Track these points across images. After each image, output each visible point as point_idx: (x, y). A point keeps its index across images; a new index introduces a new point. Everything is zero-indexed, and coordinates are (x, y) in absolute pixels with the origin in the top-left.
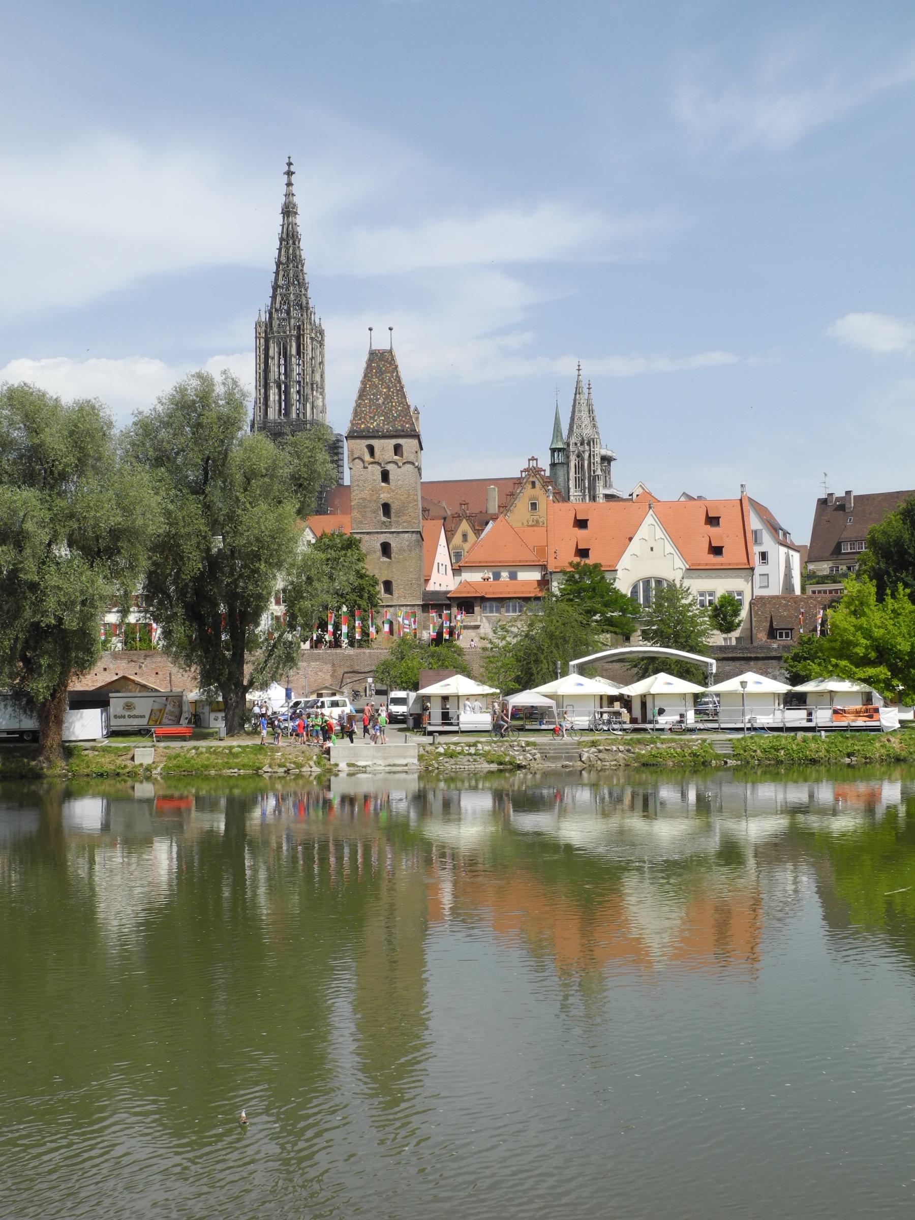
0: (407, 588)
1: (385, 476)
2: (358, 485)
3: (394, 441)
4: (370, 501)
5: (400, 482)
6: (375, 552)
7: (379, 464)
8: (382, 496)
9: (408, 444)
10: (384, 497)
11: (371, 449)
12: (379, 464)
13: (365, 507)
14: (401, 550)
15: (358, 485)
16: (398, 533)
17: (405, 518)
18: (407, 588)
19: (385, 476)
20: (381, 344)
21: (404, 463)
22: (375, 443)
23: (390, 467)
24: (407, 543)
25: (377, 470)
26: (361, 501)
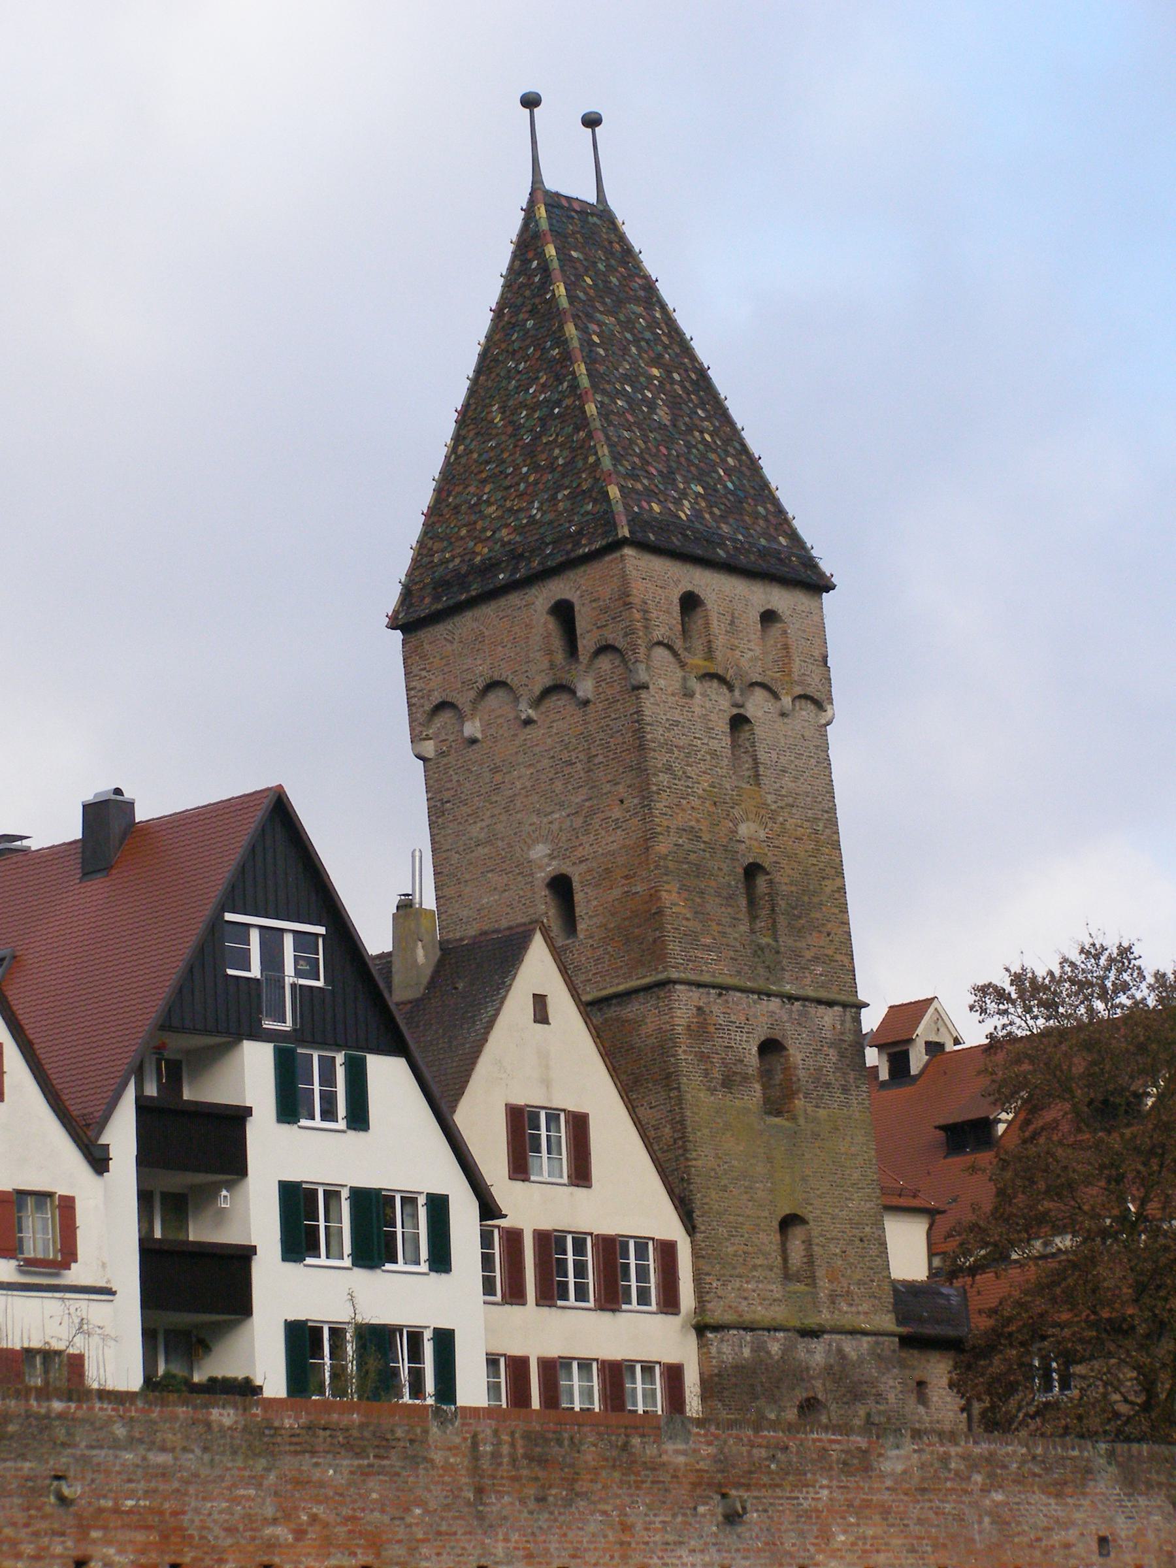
2: (669, 769)
5: (786, 780)
8: (745, 830)
15: (669, 769)
16: (806, 999)
17: (814, 939)
20: (571, 181)
22: (714, 587)
23: (757, 706)
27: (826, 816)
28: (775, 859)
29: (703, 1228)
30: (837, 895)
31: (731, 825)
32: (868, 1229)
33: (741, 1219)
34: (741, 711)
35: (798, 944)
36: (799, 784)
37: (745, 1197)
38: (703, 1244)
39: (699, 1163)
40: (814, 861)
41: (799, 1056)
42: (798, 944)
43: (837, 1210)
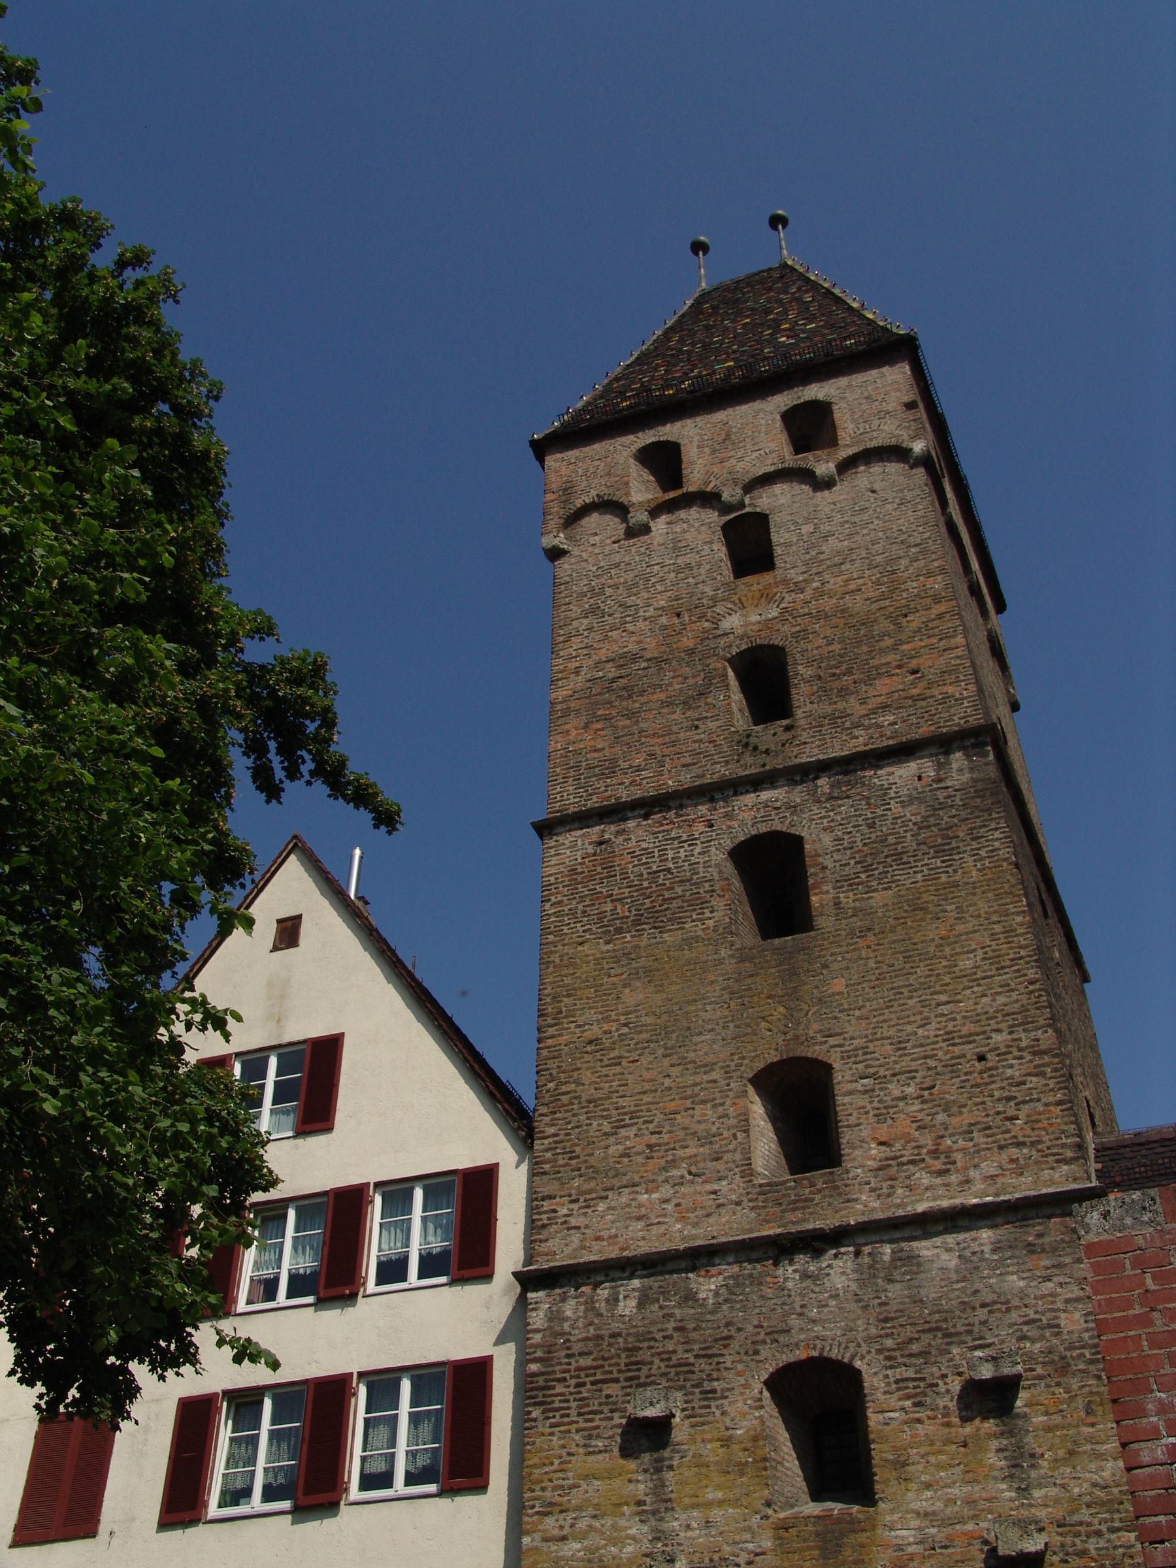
0: (950, 1089)
1: (750, 545)
3: (782, 401)
4: (659, 661)
6: (699, 903)
7: (707, 499)
9: (868, 404)
10: (742, 622)
11: (664, 462)
12: (707, 499)
13: (629, 692)
14: (878, 858)
15: (594, 611)
18: (950, 1089)
19: (750, 545)
21: (847, 465)
24: (911, 814)
25: (700, 531)
26: (611, 671)
27: (913, 550)
28: (798, 628)
29: (552, 1130)
30: (936, 623)
31: (707, 625)
32: (997, 1038)
33: (646, 1098)
34: (747, 510)
35: (841, 705)
36: (857, 538)
37: (666, 1062)
38: (548, 1155)
39: (562, 1040)
40: (887, 602)
41: (827, 839)
42: (841, 705)
43: (909, 1028)
